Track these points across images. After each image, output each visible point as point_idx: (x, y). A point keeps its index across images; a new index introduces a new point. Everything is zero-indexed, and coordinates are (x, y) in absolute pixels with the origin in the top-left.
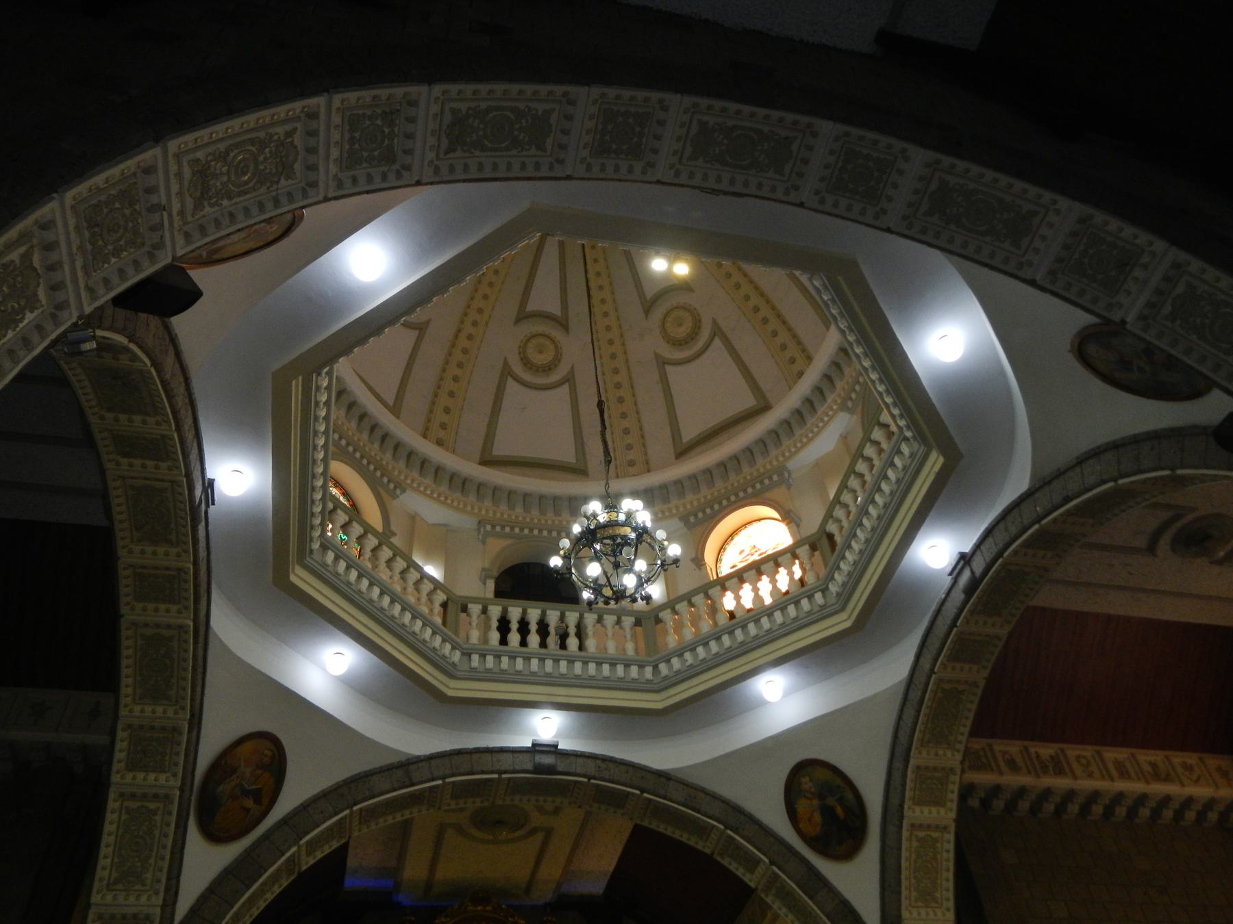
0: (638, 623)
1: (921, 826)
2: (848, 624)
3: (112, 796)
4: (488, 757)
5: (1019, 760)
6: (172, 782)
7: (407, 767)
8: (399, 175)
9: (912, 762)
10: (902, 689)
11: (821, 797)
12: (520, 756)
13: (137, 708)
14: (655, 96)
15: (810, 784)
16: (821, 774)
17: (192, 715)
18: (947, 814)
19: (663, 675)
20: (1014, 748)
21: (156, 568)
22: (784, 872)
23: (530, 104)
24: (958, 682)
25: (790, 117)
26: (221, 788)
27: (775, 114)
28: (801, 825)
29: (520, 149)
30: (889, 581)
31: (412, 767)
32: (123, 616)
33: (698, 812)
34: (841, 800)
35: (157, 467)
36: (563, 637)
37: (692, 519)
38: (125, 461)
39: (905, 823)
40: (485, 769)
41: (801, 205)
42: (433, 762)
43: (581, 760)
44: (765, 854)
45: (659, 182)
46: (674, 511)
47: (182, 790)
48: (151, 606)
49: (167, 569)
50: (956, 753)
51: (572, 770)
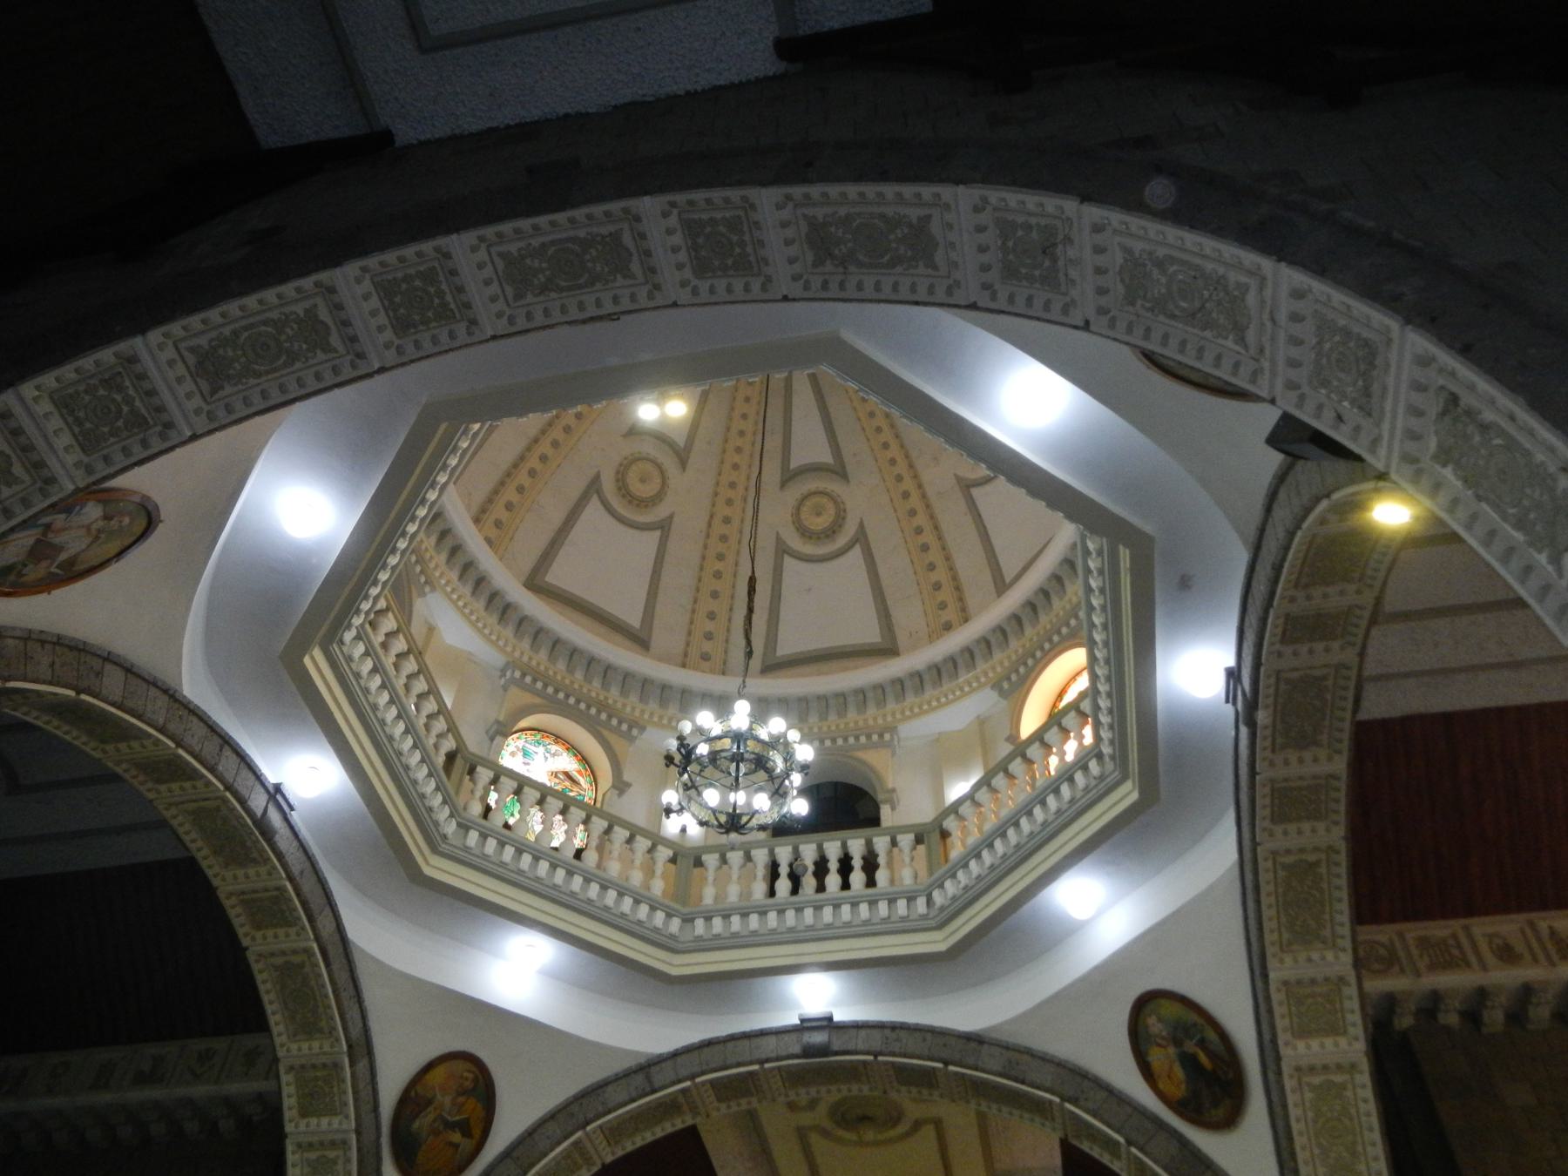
0: (919, 840)
1: (1312, 1069)
2: (1135, 796)
3: (290, 1148)
4: (746, 1042)
5: (1519, 947)
6: (345, 1126)
7: (647, 1069)
8: (163, 436)
9: (1272, 975)
10: (1236, 872)
11: (1177, 1042)
12: (786, 1037)
13: (294, 1047)
14: (427, 247)
15: (1160, 1025)
16: (1170, 1010)
17: (350, 1047)
18: (1352, 1046)
20: (1509, 926)
21: (255, 891)
22: (1146, 1154)
23: (283, 310)
24: (1302, 850)
25: (598, 210)
26: (416, 1125)
27: (579, 213)
28: (1161, 1086)
29: (304, 360)
30: (1155, 727)
31: (654, 1070)
32: (247, 949)
33: (1023, 1082)
34: (1202, 1043)
35: (194, 787)
36: (795, 879)
37: (1006, 685)
38: (163, 788)
39: (1286, 1069)
40: (740, 1060)
41: (675, 305)
42: (679, 1059)
43: (863, 1033)
44: (1118, 1131)
45: (494, 338)
46: (983, 680)
47: (358, 1132)
48: (270, 933)
49: (266, 890)
50: (1341, 955)
51: (851, 1047)
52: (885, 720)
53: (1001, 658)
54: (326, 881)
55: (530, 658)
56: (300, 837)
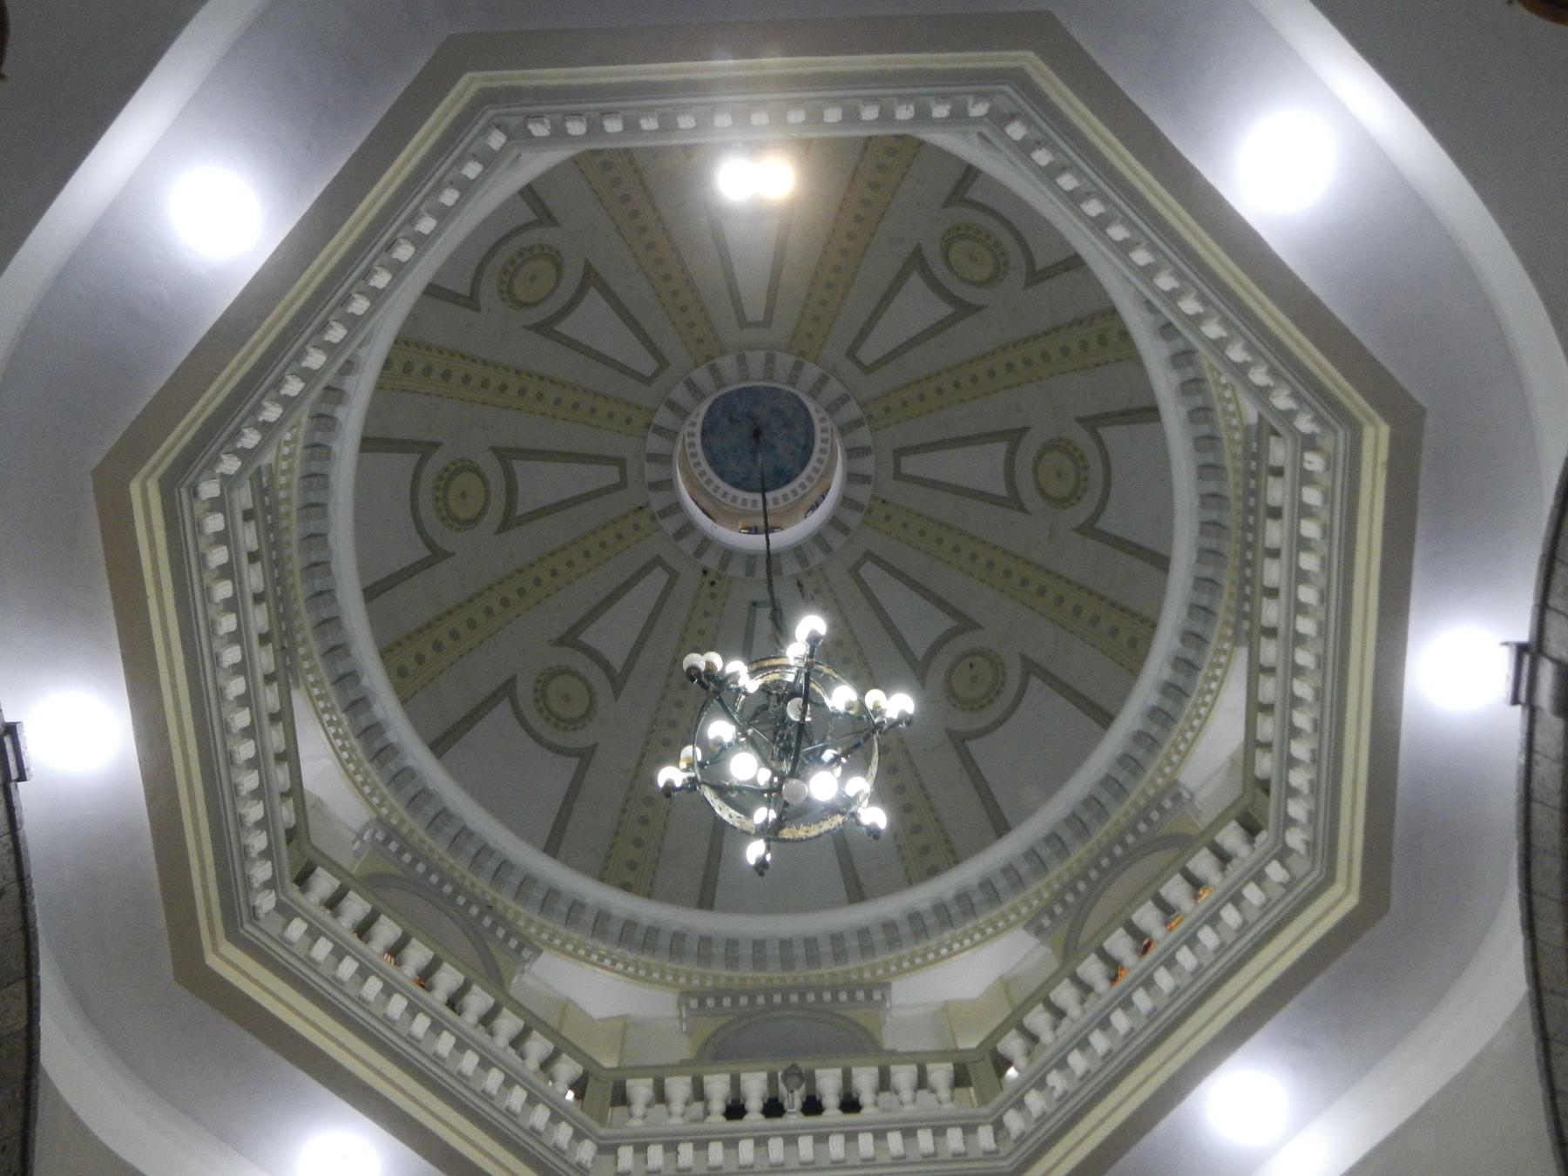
2: (1352, 900)
10: (1527, 1020)
19: (1014, 1135)
37: (1046, 922)
52: (874, 973)
53: (1039, 890)
54: (36, 938)
55: (402, 821)
56: (20, 833)
